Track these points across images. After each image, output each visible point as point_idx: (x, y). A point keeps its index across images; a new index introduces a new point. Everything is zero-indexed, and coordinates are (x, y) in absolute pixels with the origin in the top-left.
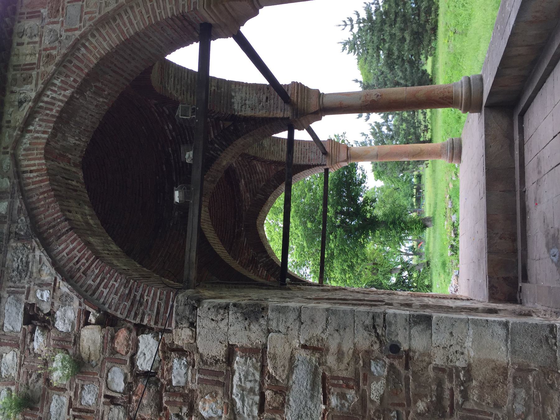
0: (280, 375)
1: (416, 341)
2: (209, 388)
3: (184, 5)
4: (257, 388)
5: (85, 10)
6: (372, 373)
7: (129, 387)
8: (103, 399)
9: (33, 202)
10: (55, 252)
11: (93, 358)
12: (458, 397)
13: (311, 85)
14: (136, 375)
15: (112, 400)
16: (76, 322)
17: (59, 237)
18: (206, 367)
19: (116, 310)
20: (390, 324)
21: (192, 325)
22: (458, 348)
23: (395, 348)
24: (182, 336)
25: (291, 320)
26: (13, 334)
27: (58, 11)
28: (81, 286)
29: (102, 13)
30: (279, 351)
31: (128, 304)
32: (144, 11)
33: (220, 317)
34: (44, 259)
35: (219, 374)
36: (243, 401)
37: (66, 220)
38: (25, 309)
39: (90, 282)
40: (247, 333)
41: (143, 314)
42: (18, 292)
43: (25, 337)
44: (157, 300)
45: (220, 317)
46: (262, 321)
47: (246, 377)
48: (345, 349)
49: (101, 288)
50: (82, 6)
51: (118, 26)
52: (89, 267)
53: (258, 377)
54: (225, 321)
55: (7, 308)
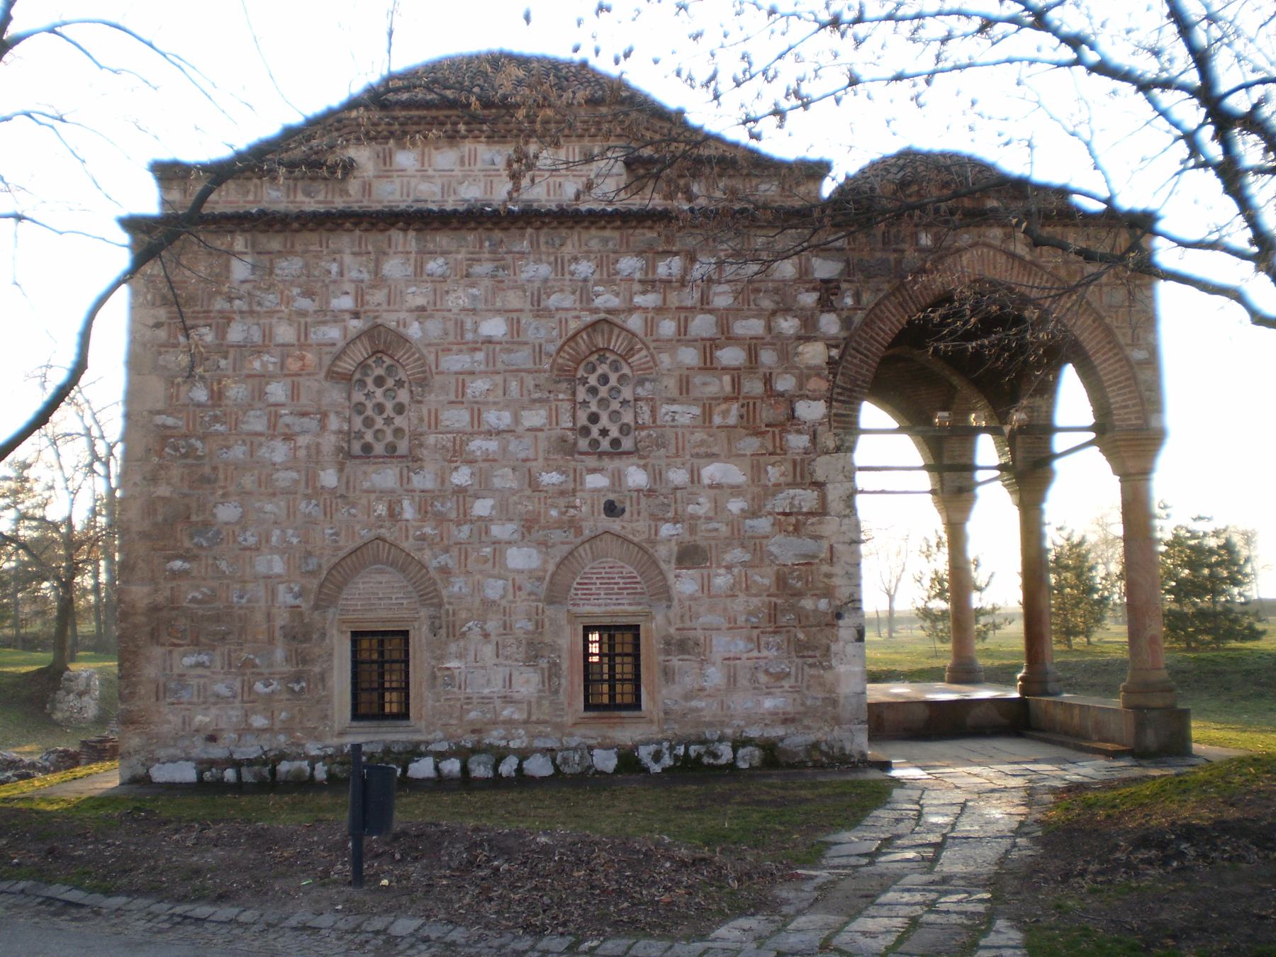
7: (782, 395)
10: (887, 302)
14: (790, 401)
15: (768, 380)
23: (839, 616)
29: (1116, 331)
34: (881, 295)
43: (811, 282)
47: (803, 500)
49: (859, 356)
51: (1103, 347)
53: (804, 510)
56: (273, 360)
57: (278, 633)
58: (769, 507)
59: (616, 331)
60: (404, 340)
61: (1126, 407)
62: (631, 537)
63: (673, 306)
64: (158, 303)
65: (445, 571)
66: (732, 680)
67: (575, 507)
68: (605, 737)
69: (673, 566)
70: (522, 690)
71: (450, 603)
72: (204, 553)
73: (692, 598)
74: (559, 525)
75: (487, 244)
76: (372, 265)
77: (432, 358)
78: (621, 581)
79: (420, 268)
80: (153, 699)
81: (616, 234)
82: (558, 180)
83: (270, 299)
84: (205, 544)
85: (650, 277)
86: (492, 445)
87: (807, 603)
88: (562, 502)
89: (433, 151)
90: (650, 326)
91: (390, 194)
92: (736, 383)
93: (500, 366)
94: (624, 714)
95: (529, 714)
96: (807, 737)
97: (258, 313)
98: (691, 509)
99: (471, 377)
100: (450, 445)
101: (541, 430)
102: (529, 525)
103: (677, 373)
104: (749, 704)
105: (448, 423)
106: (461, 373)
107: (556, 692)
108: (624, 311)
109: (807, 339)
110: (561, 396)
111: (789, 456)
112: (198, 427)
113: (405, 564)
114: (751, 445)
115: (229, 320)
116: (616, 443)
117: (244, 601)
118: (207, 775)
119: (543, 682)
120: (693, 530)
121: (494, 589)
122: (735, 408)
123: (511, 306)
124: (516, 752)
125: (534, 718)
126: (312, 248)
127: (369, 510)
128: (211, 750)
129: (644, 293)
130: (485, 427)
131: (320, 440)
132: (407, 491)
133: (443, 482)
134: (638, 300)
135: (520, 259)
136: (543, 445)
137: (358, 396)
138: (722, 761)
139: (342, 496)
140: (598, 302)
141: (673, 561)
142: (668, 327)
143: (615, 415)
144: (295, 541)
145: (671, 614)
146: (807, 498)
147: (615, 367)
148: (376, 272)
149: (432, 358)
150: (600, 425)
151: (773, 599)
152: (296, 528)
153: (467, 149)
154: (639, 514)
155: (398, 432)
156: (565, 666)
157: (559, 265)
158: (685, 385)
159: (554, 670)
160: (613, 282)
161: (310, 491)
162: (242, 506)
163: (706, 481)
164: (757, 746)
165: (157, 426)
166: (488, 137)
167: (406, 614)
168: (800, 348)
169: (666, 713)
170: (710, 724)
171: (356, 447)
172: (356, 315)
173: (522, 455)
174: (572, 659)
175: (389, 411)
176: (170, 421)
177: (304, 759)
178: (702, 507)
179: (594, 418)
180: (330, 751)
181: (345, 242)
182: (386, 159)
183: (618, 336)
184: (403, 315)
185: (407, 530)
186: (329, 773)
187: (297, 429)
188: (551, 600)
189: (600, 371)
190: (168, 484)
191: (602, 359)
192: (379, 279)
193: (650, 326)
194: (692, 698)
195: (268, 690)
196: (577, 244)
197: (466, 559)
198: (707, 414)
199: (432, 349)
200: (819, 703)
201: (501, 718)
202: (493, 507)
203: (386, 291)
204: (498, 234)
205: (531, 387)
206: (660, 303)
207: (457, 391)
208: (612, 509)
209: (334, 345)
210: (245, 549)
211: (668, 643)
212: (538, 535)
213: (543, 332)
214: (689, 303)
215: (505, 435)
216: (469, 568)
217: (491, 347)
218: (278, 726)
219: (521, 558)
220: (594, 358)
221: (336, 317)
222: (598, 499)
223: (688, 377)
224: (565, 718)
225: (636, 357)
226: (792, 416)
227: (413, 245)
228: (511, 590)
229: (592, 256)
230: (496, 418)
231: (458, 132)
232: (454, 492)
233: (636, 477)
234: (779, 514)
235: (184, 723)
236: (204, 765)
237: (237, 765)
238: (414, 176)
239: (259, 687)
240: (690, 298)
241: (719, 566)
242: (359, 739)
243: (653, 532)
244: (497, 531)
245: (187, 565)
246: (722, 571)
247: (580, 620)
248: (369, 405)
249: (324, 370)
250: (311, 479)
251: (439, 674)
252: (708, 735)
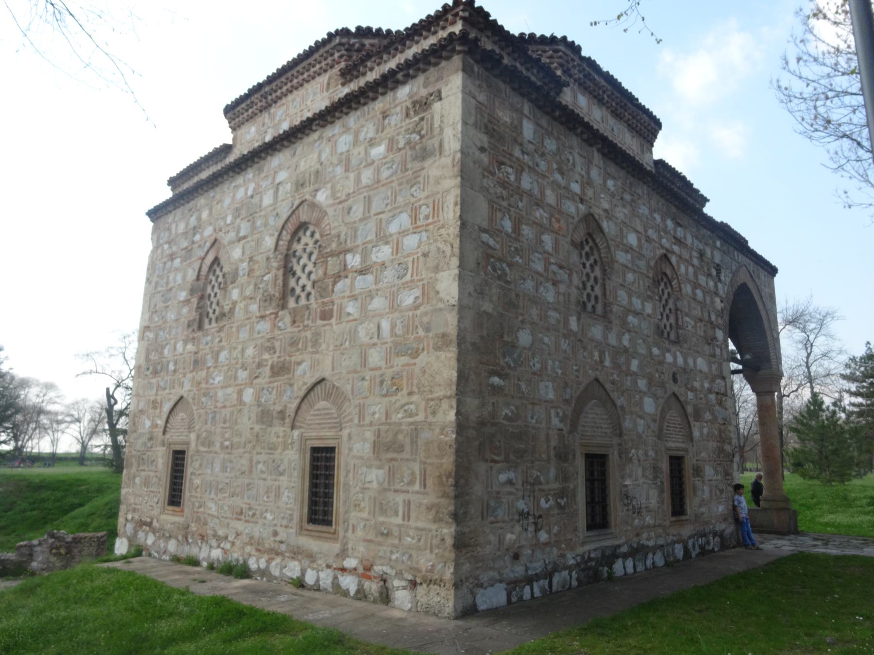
57: (552, 453)
80: (480, 519)
144: (560, 372)
236: (513, 585)
245: (502, 383)
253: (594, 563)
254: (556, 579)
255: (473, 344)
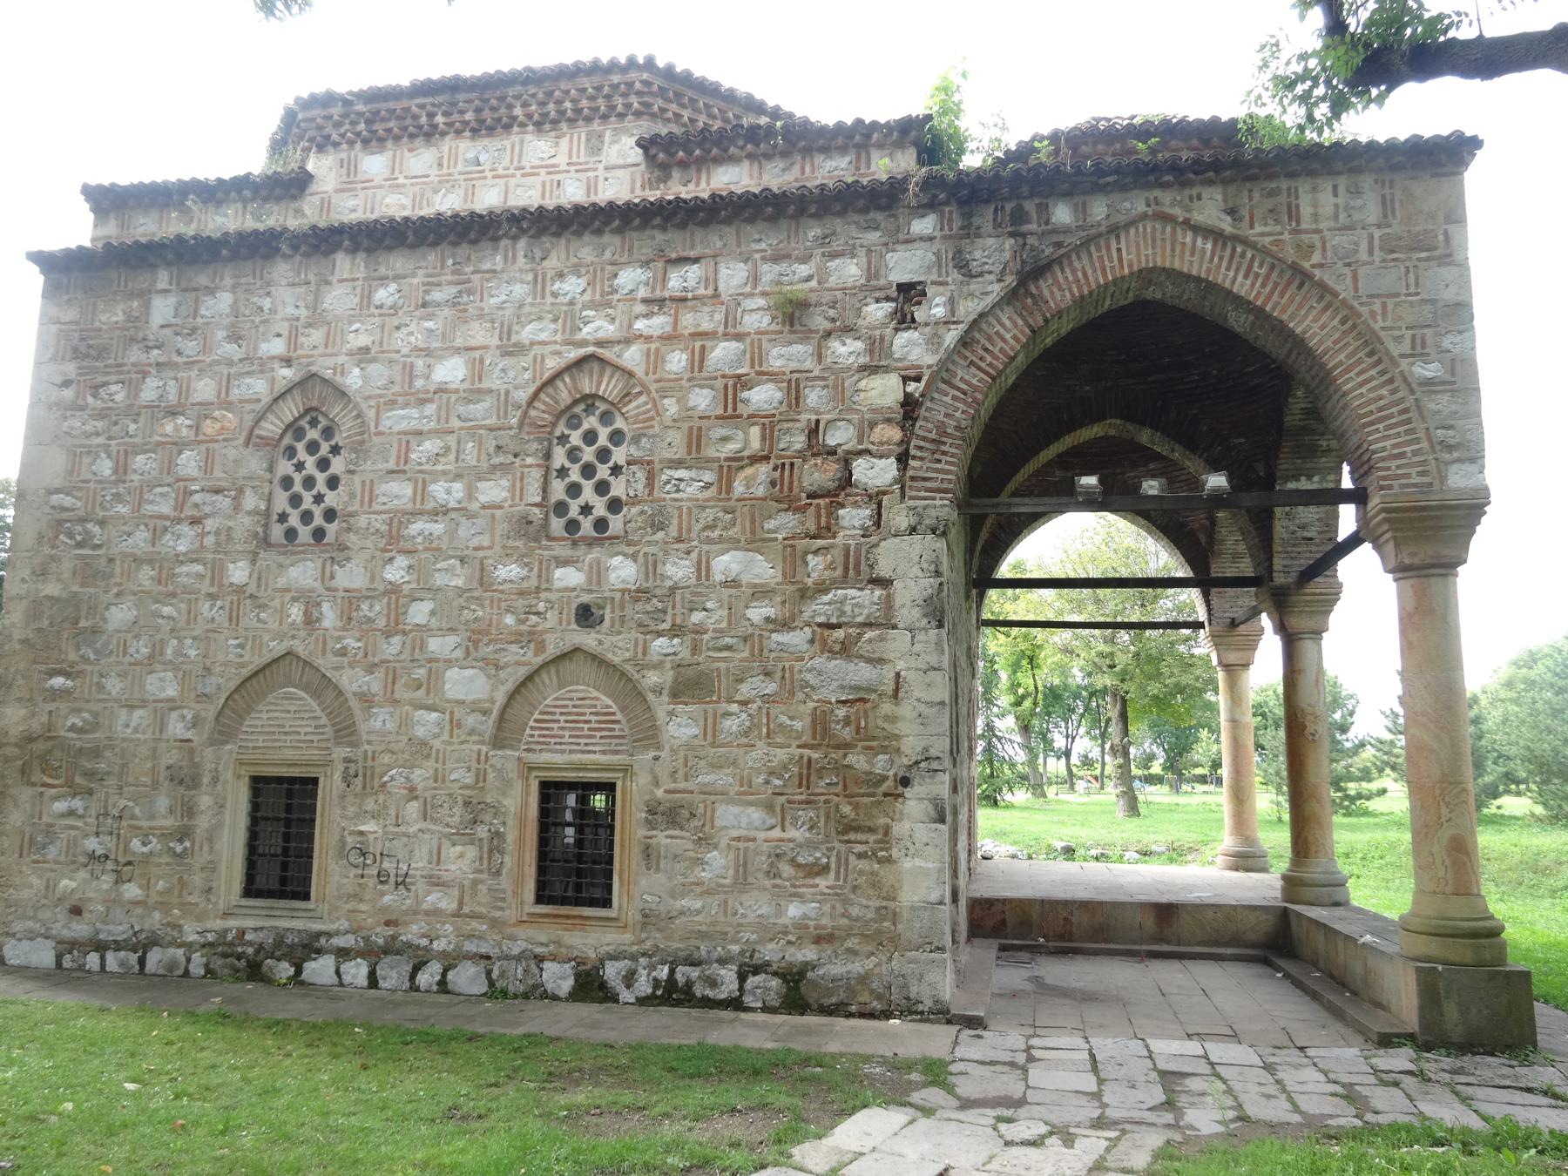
0: (863, 647)
1: (914, 805)
2: (840, 560)
3: (1389, 469)
4: (845, 620)
5: (1390, 303)
6: (876, 755)
7: (832, 452)
8: (814, 417)
9: (1071, 264)
10: (999, 312)
11: (862, 395)
12: (859, 848)
13: (1339, 617)
15: (813, 431)
16: (906, 363)
17: (1020, 315)
18: (863, 553)
19: (925, 419)
20: (932, 777)
21: (913, 530)
22: (912, 850)
23: (905, 782)
24: (899, 518)
25: (928, 658)
26: (882, 272)
27: (1393, 251)
28: (954, 362)
29: (1382, 334)
30: (889, 645)
31: (933, 436)
32: (1382, 403)
33: (925, 566)
34: (989, 300)
35: (858, 573)
36: (829, 604)
37: (1046, 321)
38: (920, 283)
39: (960, 373)
40: (909, 604)
41: (921, 459)
42: (940, 267)
44: (941, 476)
45: (925, 566)
46: (925, 621)
47: (856, 605)
48: (899, 725)
50: (1397, 295)
51: (1360, 361)
52: (979, 368)
53: (859, 619)
54: (920, 574)
55: (918, 253)
56: (188, 422)
57: (163, 773)
58: (806, 616)
59: (608, 371)
60: (342, 394)
61: (1402, 455)
62: (610, 656)
63: (686, 332)
64: (69, 355)
65: (367, 700)
66: (743, 869)
67: (537, 613)
68: (557, 943)
69: (665, 698)
70: (453, 867)
71: (369, 742)
72: (89, 668)
73: (688, 746)
74: (516, 638)
75: (450, 262)
76: (310, 298)
77: (372, 414)
78: (593, 718)
79: (366, 298)
81: (616, 240)
82: (557, 177)
83: (191, 347)
84: (92, 657)
85: (658, 293)
86: (438, 528)
87: (857, 760)
88: (520, 603)
89: (407, 154)
90: (655, 360)
91: (351, 210)
92: (768, 435)
93: (455, 423)
94: (588, 911)
95: (461, 904)
96: (849, 967)
97: (177, 364)
98: (697, 617)
99: (419, 438)
100: (384, 528)
101: (501, 507)
102: (476, 636)
103: (686, 425)
104: (764, 910)
105: (384, 499)
106: (405, 433)
107: (498, 873)
108: (619, 342)
109: (871, 370)
110: (529, 460)
111: (839, 540)
112: (98, 509)
113: (322, 687)
114: (783, 524)
115: (145, 374)
116: (601, 524)
117: (129, 731)
118: (67, 962)
119: (481, 859)
120: (695, 650)
121: (427, 722)
122: (763, 471)
123: (472, 343)
124: (444, 955)
125: (466, 910)
126: (243, 280)
127: (282, 614)
128: (74, 926)
129: (646, 316)
130: (430, 505)
131: (231, 524)
132: (328, 589)
133: (372, 579)
134: (640, 325)
135: (488, 280)
136: (502, 528)
137: (285, 467)
138: (723, 996)
139: (251, 596)
140: (586, 331)
141: (666, 692)
142: (677, 361)
143: (602, 488)
144: (193, 653)
145: (657, 769)
146: (865, 600)
147: (606, 418)
148: (314, 307)
149: (372, 414)
150: (581, 501)
151: (806, 752)
152: (194, 638)
153: (446, 148)
154: (623, 623)
155: (330, 515)
156: (511, 837)
157: (539, 283)
158: (696, 440)
159: (496, 842)
160: (609, 305)
161: (213, 590)
162: (138, 608)
163: (718, 577)
164: (775, 974)
165: (53, 507)
166: (473, 130)
167: (314, 754)
168: (863, 384)
169: (645, 916)
170: (703, 936)
171: (277, 532)
172: (287, 362)
173: (475, 542)
174: (522, 825)
175: (321, 486)
176: (68, 501)
177: (179, 946)
178: (711, 617)
179: (574, 490)
180: (211, 937)
181: (282, 270)
182: (350, 167)
183: (612, 377)
184: (341, 359)
185: (325, 642)
186: (206, 965)
187: (207, 509)
188: (498, 742)
189: (586, 426)
190: (58, 580)
191: (590, 409)
192: (317, 317)
193: (655, 360)
194: (683, 896)
195: (145, 849)
196: (563, 256)
197: (394, 683)
198: (725, 483)
199: (372, 403)
200: (871, 915)
201: (425, 906)
202: (433, 613)
203: (326, 328)
204: (464, 250)
205: (492, 450)
206: (668, 329)
207: (399, 457)
208: (586, 616)
209: (258, 401)
210: (137, 664)
211: (651, 812)
212: (486, 651)
213: (512, 374)
214: (706, 326)
215: (453, 515)
216: (397, 695)
217: (445, 396)
218: (153, 899)
219: (464, 684)
220: (578, 409)
221: (262, 366)
222: (569, 603)
223: (700, 429)
224: (508, 912)
225: (634, 404)
226: (846, 481)
227: (361, 273)
228: (448, 727)
229: (583, 271)
230: (445, 492)
231: (436, 126)
232: (384, 594)
233: (623, 570)
234: (820, 625)
235: (47, 887)
237: (101, 947)
238: (380, 187)
239: (136, 844)
240: (707, 320)
241: (730, 701)
242: (249, 923)
243: (640, 649)
244: (435, 645)
245: (70, 683)
246: (734, 708)
247: (535, 773)
248: (298, 478)
249: (244, 434)
250: (217, 572)
251: (349, 839)
252: (703, 953)
253: (250, 950)
254: (154, 958)
255: (23, 642)
